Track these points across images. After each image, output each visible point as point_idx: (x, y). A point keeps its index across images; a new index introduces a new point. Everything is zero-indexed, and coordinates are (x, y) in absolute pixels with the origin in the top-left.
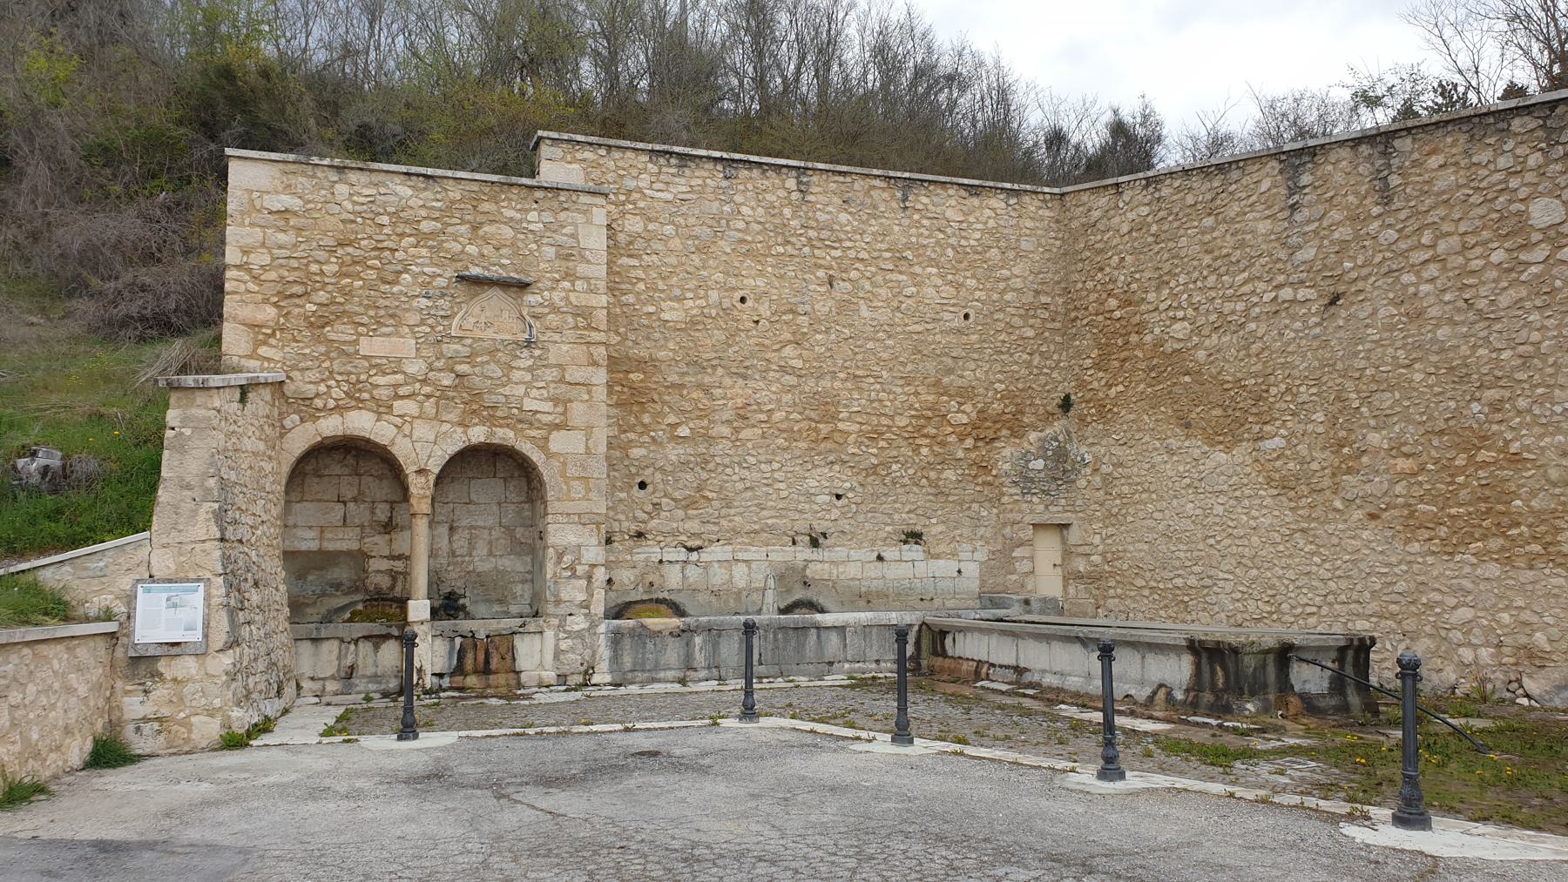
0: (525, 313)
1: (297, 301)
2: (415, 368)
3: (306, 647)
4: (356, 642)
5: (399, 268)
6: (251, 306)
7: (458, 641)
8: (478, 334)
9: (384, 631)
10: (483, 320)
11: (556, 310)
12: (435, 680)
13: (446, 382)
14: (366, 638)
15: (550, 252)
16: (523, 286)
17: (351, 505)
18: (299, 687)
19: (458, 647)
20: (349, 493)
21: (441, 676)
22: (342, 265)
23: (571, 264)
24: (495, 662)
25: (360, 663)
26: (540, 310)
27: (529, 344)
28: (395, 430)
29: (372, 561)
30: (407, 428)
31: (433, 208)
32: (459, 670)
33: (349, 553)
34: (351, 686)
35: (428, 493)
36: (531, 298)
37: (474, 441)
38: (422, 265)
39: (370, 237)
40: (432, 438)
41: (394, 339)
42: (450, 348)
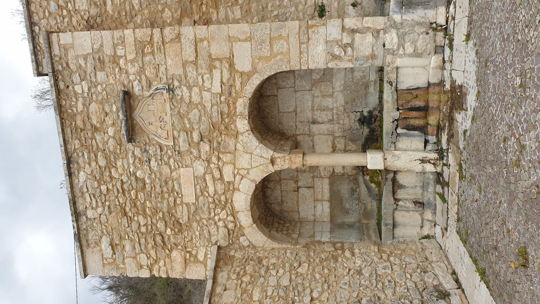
0: (148, 94)
1: (166, 239)
2: (200, 168)
3: (399, 232)
4: (396, 200)
5: (133, 178)
6: (173, 264)
7: (399, 131)
8: (169, 127)
9: (389, 183)
10: (158, 124)
11: (142, 71)
12: (429, 147)
13: (207, 148)
14: (394, 193)
15: (101, 76)
16: (128, 97)
17: (300, 184)
18: (427, 237)
19: (405, 131)
20: (293, 185)
21: (426, 142)
22: (138, 214)
23: (107, 59)
24: (419, 103)
25: (412, 197)
26: (144, 83)
27: (170, 90)
28: (245, 180)
29: (336, 171)
30: (243, 172)
31: (89, 158)
32: (423, 129)
33: (331, 184)
34: (429, 203)
35: (287, 157)
36: (137, 90)
37: (247, 127)
38: (128, 164)
39: (117, 197)
40: (248, 156)
41: (182, 181)
42: (183, 145)
